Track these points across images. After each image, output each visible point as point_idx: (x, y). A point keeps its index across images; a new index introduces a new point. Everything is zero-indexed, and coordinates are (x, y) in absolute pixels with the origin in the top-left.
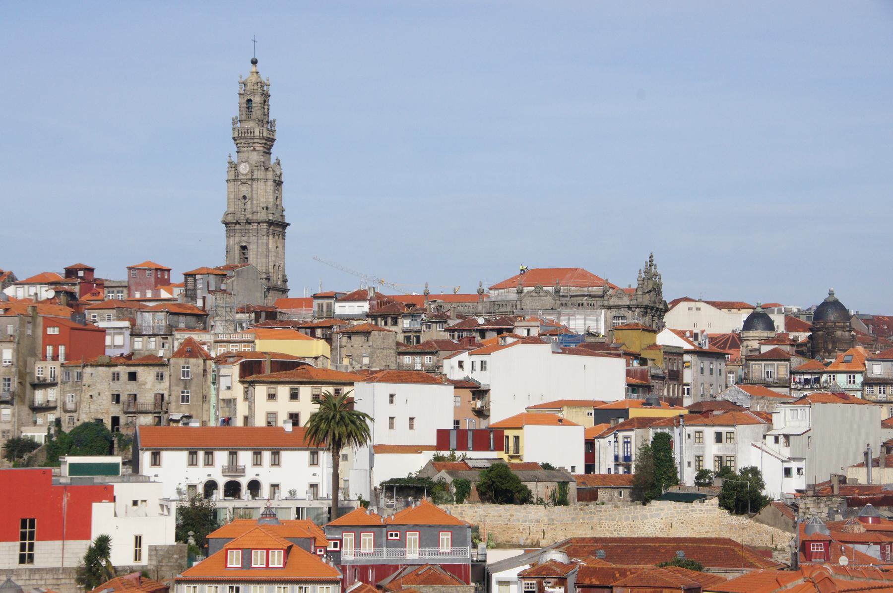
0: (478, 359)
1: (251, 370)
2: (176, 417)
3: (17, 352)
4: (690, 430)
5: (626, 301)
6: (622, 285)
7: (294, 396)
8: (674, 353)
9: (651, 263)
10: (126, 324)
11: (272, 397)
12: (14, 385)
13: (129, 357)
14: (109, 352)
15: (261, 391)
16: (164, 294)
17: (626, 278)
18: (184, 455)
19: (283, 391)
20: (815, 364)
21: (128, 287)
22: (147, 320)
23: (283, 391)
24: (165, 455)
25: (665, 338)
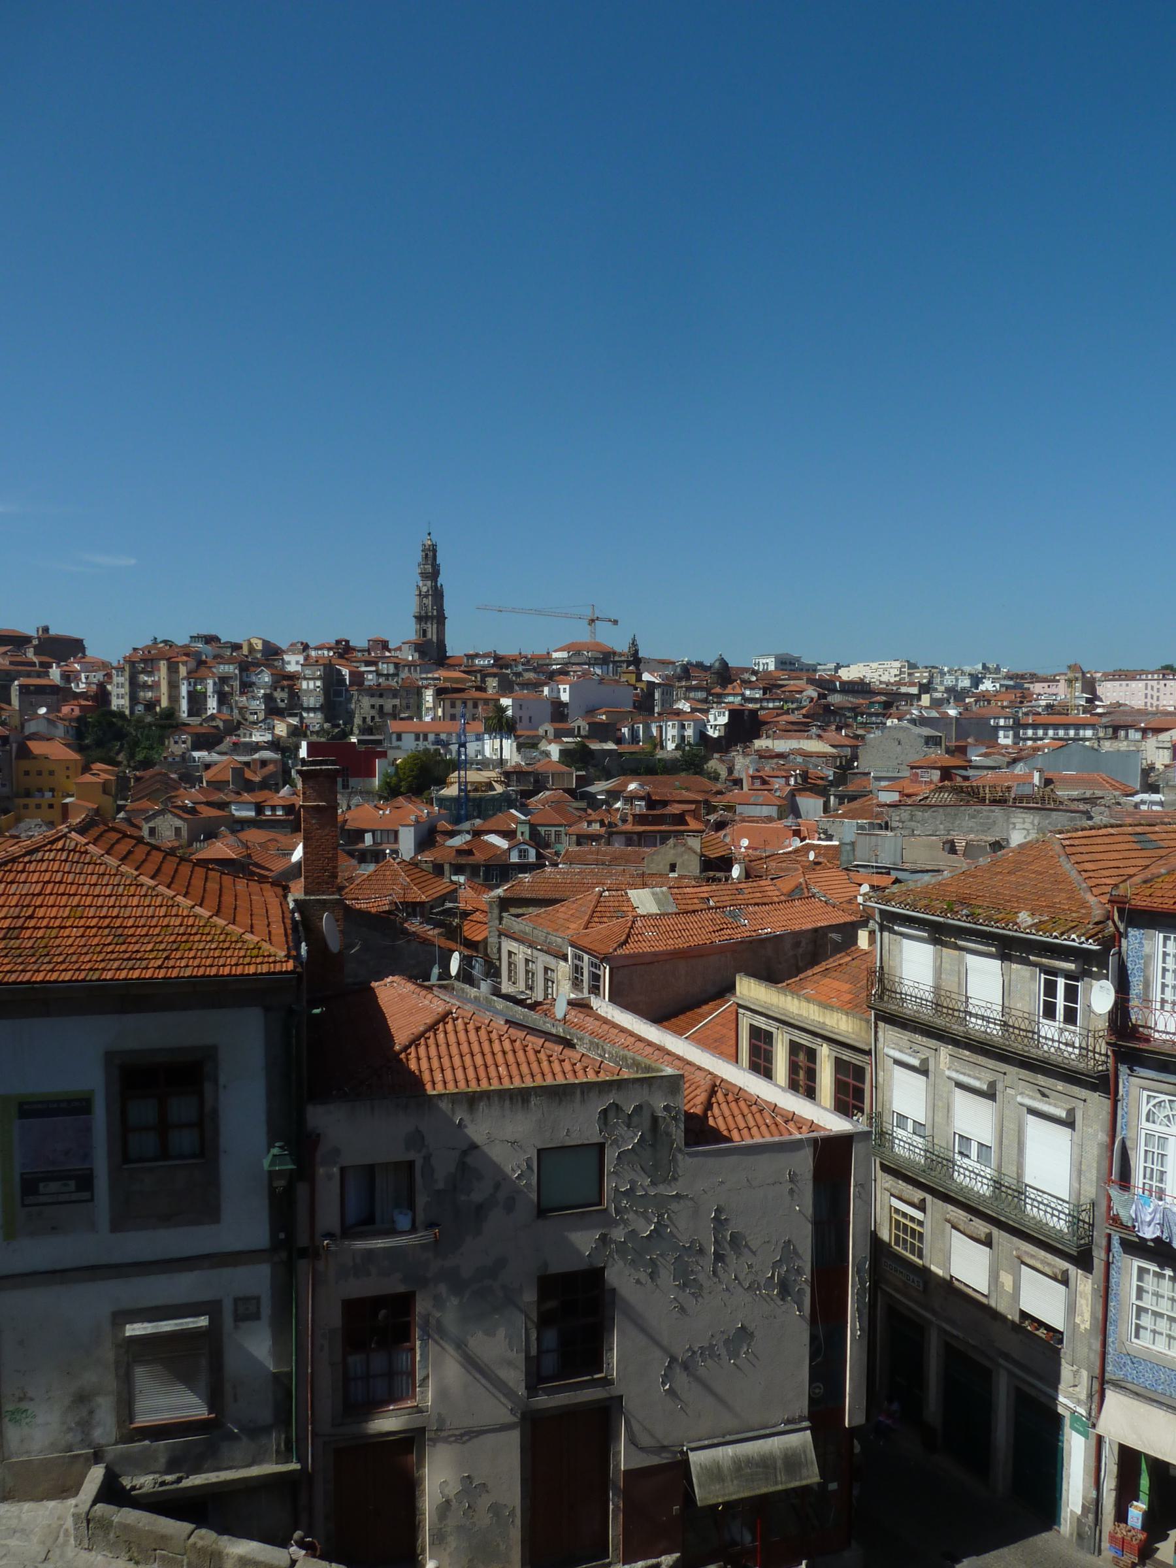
0: (561, 687)
1: (440, 693)
2: (403, 715)
3: (324, 684)
4: (670, 723)
5: (623, 658)
6: (618, 649)
7: (465, 703)
8: (650, 684)
9: (634, 640)
10: (373, 669)
11: (453, 706)
12: (321, 700)
13: (379, 685)
14: (366, 683)
15: (448, 703)
16: (387, 654)
17: (621, 646)
18: (413, 736)
19: (458, 703)
20: (718, 690)
21: (369, 651)
22: (384, 668)
23: (458, 703)
24: (404, 735)
25: (646, 677)
